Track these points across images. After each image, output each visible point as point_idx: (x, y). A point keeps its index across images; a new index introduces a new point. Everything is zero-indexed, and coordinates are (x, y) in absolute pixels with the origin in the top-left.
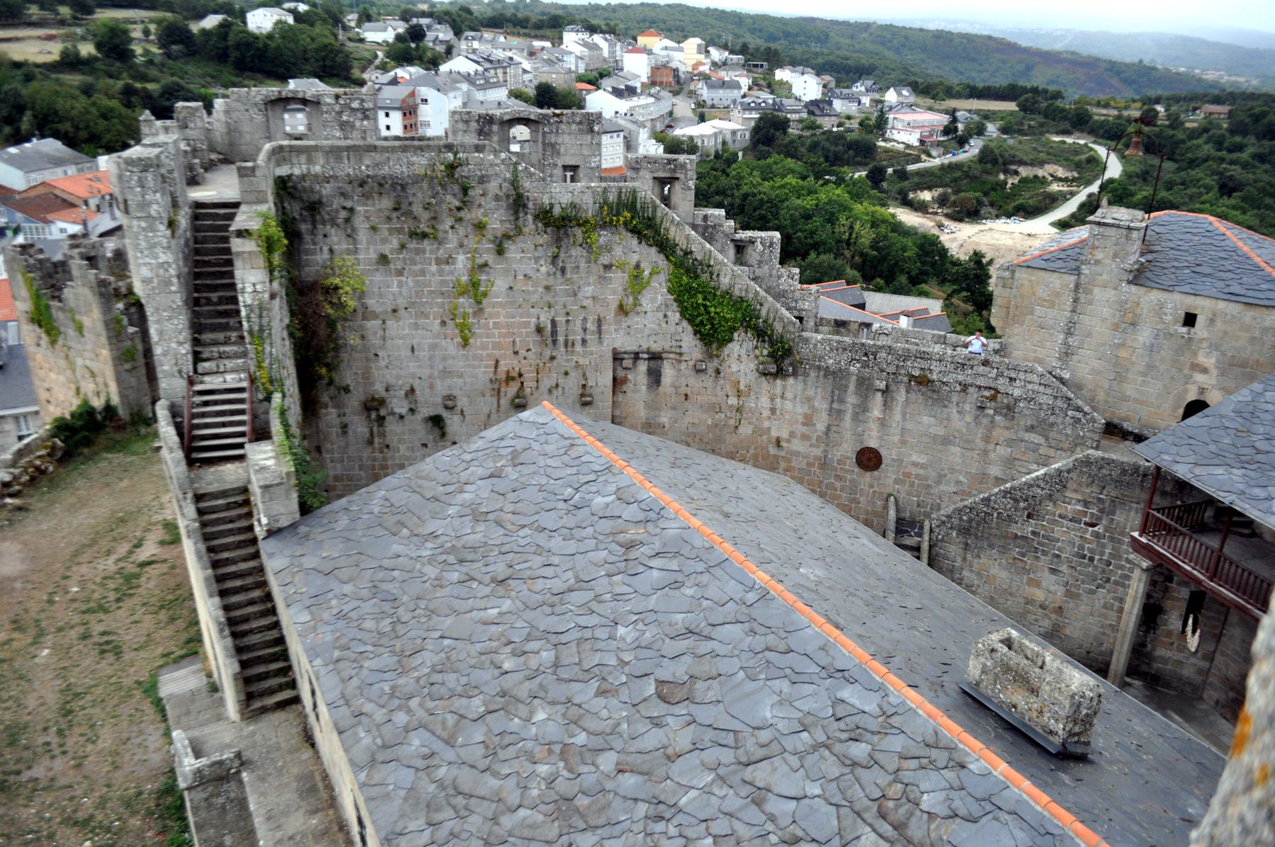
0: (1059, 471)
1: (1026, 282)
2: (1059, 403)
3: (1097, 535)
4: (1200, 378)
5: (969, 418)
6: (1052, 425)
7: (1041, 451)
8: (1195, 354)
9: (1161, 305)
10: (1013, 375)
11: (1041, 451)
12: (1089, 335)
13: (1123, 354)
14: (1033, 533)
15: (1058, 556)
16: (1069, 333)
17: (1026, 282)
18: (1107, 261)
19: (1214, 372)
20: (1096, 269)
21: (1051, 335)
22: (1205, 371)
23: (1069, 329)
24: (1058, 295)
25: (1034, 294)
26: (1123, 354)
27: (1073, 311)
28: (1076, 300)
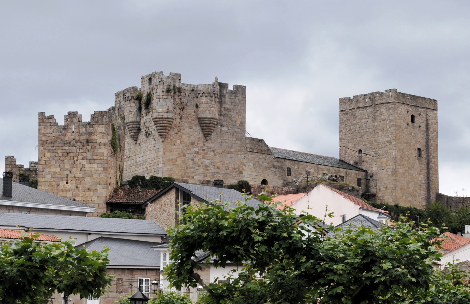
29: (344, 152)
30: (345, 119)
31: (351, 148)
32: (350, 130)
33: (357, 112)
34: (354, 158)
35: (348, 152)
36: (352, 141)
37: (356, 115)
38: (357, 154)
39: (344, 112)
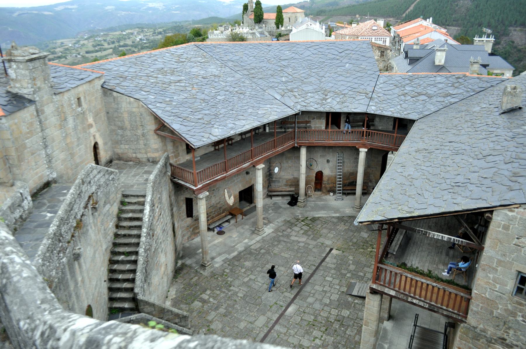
0: (151, 200)
1: (14, 127)
4: (93, 130)
5: (93, 228)
7: (111, 213)
8: (87, 120)
9: (70, 100)
10: (89, 179)
12: (53, 141)
13: (68, 141)
16: (46, 147)
17: (14, 127)
18: (43, 85)
19: (94, 124)
20: (40, 93)
21: (39, 155)
22: (91, 126)
23: (45, 144)
24: (31, 124)
25: (21, 133)
26: (68, 141)
27: (42, 130)
28: (40, 122)
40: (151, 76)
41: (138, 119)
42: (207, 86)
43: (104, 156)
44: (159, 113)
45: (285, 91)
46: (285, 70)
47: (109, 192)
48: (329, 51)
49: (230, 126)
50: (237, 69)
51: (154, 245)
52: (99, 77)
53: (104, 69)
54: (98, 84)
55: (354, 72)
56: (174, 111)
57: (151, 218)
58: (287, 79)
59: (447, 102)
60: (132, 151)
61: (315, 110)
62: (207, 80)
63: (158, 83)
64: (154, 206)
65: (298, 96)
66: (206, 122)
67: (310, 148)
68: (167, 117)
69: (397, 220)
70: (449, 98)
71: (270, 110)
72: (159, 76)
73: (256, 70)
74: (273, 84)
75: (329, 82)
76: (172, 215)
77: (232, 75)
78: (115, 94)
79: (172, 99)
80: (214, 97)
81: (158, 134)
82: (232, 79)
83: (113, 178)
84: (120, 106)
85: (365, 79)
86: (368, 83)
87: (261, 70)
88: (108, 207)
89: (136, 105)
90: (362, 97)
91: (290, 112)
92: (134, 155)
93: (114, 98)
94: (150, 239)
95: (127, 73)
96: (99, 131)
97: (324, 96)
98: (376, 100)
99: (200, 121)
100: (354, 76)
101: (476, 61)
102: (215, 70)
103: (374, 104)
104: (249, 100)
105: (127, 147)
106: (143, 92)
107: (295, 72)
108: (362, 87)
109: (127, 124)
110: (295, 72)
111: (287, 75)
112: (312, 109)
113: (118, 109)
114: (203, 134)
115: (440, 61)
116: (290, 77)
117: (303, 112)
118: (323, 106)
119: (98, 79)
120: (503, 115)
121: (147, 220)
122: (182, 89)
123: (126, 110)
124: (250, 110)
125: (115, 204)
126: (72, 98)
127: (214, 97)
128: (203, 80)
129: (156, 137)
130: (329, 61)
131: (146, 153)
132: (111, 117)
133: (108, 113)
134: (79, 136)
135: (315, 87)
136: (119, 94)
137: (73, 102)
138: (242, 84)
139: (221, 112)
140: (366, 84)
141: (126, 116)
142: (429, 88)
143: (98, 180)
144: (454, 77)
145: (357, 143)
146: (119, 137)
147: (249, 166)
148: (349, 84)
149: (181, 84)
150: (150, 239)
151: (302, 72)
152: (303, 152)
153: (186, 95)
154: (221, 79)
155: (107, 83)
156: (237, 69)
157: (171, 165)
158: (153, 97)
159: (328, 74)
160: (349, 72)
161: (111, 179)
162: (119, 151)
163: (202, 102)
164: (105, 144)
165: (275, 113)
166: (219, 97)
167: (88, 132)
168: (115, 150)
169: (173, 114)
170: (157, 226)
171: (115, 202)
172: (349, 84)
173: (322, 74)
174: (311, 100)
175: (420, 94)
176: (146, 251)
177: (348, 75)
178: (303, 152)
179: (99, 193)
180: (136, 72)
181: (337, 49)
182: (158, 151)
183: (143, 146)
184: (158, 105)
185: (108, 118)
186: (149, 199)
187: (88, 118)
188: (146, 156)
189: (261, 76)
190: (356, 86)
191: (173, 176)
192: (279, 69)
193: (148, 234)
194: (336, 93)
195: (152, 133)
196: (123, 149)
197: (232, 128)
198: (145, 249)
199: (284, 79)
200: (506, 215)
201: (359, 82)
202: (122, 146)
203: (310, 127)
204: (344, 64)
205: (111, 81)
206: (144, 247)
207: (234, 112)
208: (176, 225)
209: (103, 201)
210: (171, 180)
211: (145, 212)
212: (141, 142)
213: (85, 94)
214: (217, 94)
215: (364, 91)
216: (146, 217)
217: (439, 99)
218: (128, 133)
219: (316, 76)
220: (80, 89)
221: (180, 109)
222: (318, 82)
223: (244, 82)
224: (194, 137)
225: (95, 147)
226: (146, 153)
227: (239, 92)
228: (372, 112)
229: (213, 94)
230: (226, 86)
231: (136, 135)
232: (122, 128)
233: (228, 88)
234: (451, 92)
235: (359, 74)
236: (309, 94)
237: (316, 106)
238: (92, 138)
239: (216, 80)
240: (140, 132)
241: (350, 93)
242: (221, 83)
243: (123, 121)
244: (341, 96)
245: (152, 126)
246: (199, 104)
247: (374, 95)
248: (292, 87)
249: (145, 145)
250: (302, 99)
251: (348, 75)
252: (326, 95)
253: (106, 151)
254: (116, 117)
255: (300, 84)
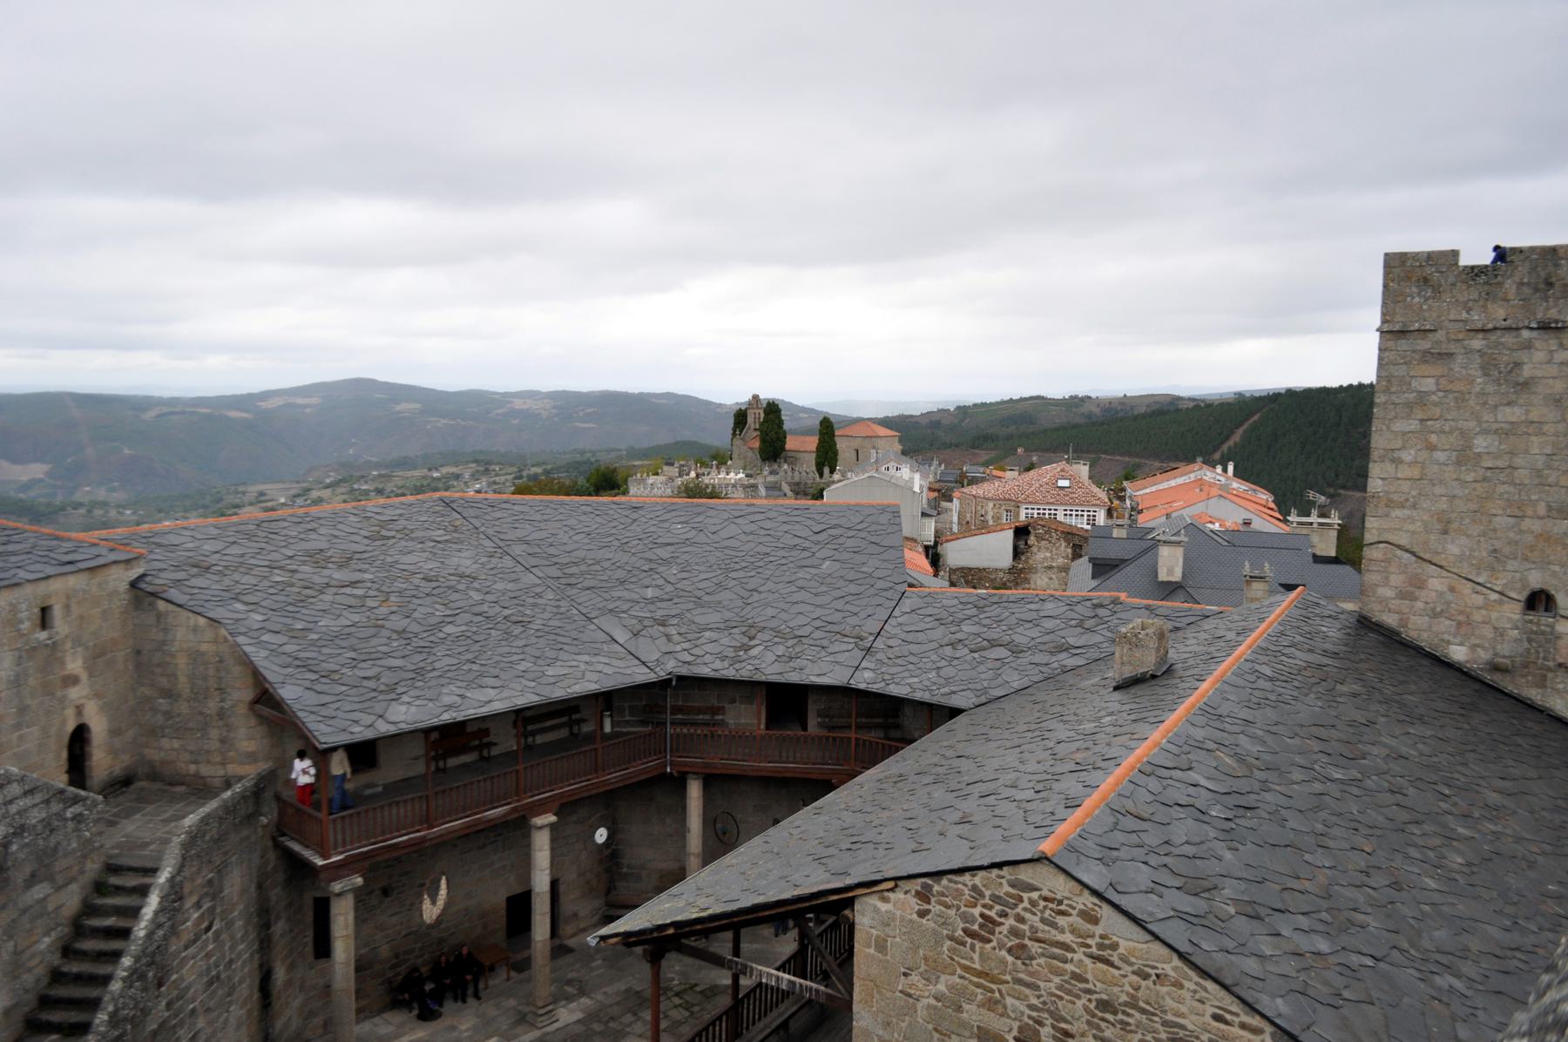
0: (171, 880)
2: (55, 807)
3: (217, 935)
4: (74, 693)
6: (55, 849)
7: (50, 907)
8: (63, 663)
11: (50, 907)
14: (169, 1005)
15: (193, 1011)
19: (84, 677)
22: (73, 680)
29: (1396, 580)
30: (1429, 384)
31: (1465, 570)
32: (1464, 456)
33: (1539, 356)
34: (1488, 632)
35: (1437, 583)
36: (1475, 530)
37: (1527, 372)
38: (1513, 612)
39: (1424, 344)
40: (280, 568)
41: (211, 672)
42: (429, 600)
43: (101, 762)
44: (259, 657)
45: (646, 623)
46: (661, 569)
47: (55, 849)
48: (786, 527)
49: (447, 700)
50: (533, 561)
51: (160, 1011)
52: (128, 562)
53: (159, 545)
54: (120, 579)
55: (841, 583)
56: (302, 655)
57: (161, 933)
58: (658, 593)
59: (1055, 665)
60: (187, 756)
61: (712, 674)
62: (434, 584)
63: (292, 585)
64: (181, 899)
65: (677, 638)
66: (382, 688)
67: (712, 781)
68: (276, 668)
69: (671, 931)
70: (1064, 655)
71: (583, 667)
72: (306, 568)
73: (583, 568)
74: (618, 603)
75: (767, 605)
76: (265, 944)
77: (514, 576)
78: (161, 605)
79: (311, 626)
80: (438, 626)
81: (259, 716)
82: (510, 586)
83: (81, 814)
84: (170, 637)
85: (864, 602)
86: (870, 611)
87: (597, 567)
88: (40, 891)
89: (209, 635)
90: (845, 647)
91: (642, 676)
92: (193, 768)
93: (159, 616)
94: (145, 989)
95: (217, 556)
96: (98, 695)
97: (746, 640)
98: (880, 656)
99: (365, 683)
100: (838, 593)
101: (1256, 573)
102: (468, 562)
103: (872, 666)
104: (534, 640)
105: (176, 744)
106: (239, 606)
107: (685, 575)
108: (853, 621)
109: (183, 683)
110: (685, 575)
111: (661, 582)
112: (705, 671)
113: (164, 643)
114: (356, 716)
115: (1170, 571)
116: (669, 588)
117: (681, 678)
118: (737, 666)
119: (122, 566)
120: (1117, 695)
121: (142, 934)
122: (352, 602)
123: (185, 646)
124: (523, 666)
125: (74, 887)
126: (24, 606)
127: (438, 626)
128: (423, 584)
129: (253, 721)
130: (782, 553)
131: (223, 764)
132: (146, 662)
133: (138, 652)
134: (28, 701)
135: (728, 615)
136: (171, 607)
137: (23, 615)
138: (531, 600)
139: (437, 665)
140: (863, 615)
141: (182, 662)
142: (1020, 630)
143: (19, 813)
144: (1088, 604)
145: (834, 772)
146: (160, 718)
147: (505, 815)
148: (819, 612)
149: (356, 592)
150: (145, 989)
151: (703, 576)
152: (694, 790)
153: (356, 618)
154: (475, 584)
155: (148, 579)
156: (533, 561)
157: (278, 797)
158: (260, 618)
159: (770, 585)
160: (828, 580)
161: (69, 815)
162: (153, 755)
163: (394, 636)
164: (114, 732)
165: (595, 677)
166: (449, 629)
167: (59, 694)
168: (147, 751)
169: (297, 663)
170: (184, 961)
171: (73, 880)
172: (819, 612)
173: (752, 584)
174: (709, 648)
175: (994, 644)
176: (114, 1020)
177: (824, 588)
178: (694, 790)
179: (14, 847)
180: (243, 555)
181: (809, 523)
182: (256, 761)
183: (218, 745)
184: (265, 638)
185: (139, 666)
186: (163, 877)
187: (68, 659)
188: (221, 773)
189: (586, 584)
190: (837, 617)
191: (281, 829)
192: (646, 568)
193: (136, 975)
194: (777, 632)
195: (242, 709)
196: (168, 749)
197: (450, 707)
198: (113, 1015)
199: (650, 593)
200: (876, 910)
201: (848, 607)
202: (165, 742)
203: (722, 723)
204: (816, 562)
205: (163, 575)
206: (111, 1008)
207: (475, 667)
208: (280, 975)
209: (28, 870)
210: (274, 839)
211: (144, 911)
212: (214, 733)
213: (68, 598)
214: (451, 619)
215: (855, 633)
216: (143, 924)
217: (1038, 658)
218: (184, 708)
219: (738, 589)
220: (56, 585)
221: (325, 650)
222: (739, 603)
223: (539, 595)
224: (331, 722)
225: (80, 737)
226: (223, 764)
227: (514, 618)
228: (862, 686)
229: (433, 620)
230: (483, 602)
231: (201, 713)
232: (169, 694)
233: (485, 608)
234: (1071, 641)
235: (853, 588)
236: (707, 634)
237: (718, 664)
238: (70, 712)
239: (461, 587)
240: (212, 706)
241: (818, 634)
242: (472, 593)
243: (174, 675)
244: (791, 642)
245: (242, 694)
246: (385, 641)
247: (879, 644)
248: (665, 612)
249: (223, 741)
250: (686, 646)
251: (824, 588)
252: (751, 638)
253: (113, 752)
254: (158, 665)
255: (691, 606)
